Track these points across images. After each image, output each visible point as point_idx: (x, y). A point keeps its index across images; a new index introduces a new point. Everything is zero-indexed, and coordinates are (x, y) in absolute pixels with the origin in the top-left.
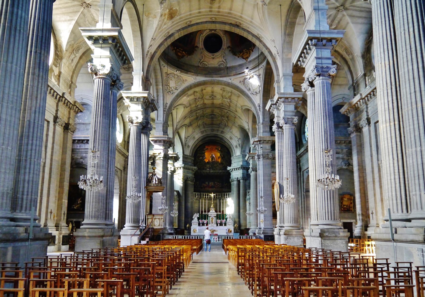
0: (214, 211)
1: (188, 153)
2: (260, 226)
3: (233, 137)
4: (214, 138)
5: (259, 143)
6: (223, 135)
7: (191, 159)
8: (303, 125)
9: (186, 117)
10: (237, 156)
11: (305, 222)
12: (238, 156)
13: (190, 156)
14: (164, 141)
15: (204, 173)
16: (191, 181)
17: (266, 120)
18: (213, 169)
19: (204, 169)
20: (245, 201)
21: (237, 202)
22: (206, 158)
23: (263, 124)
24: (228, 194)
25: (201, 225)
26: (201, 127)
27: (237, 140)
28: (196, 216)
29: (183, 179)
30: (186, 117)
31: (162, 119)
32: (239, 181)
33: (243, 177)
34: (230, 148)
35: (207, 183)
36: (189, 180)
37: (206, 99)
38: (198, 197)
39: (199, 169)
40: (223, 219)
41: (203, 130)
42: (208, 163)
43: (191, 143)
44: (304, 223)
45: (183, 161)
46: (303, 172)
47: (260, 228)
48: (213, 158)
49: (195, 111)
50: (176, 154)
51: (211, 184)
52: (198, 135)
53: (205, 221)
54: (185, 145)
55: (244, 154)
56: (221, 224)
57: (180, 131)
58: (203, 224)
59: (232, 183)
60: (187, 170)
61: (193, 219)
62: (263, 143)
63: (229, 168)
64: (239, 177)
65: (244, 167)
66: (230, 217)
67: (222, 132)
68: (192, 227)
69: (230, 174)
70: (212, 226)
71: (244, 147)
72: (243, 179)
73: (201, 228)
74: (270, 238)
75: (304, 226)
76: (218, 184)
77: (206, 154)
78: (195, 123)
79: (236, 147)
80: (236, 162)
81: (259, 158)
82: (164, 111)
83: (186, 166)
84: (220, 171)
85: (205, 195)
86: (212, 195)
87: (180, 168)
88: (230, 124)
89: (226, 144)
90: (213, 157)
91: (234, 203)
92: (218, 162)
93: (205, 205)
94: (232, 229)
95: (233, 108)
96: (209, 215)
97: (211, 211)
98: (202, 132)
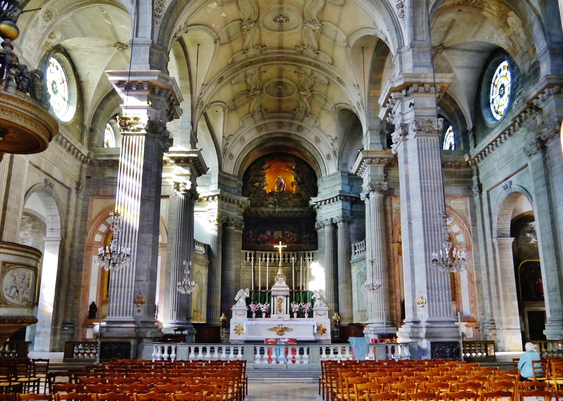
0: (284, 284)
1: (229, 168)
2: (415, 314)
3: (322, 137)
4: (280, 143)
5: (404, 92)
6: (300, 134)
7: (235, 181)
8: (484, 87)
9: (221, 79)
10: (329, 176)
11: (499, 308)
12: (333, 175)
13: (235, 176)
14: (152, 87)
15: (263, 212)
16: (236, 226)
17: (419, 37)
18: (280, 206)
19: (262, 205)
20: (349, 266)
21: (331, 269)
22: (266, 185)
23: (412, 46)
24: (311, 252)
25: (254, 315)
26: (258, 116)
27: (329, 142)
28: (242, 296)
29: (218, 220)
30: (221, 79)
31: (148, 34)
32: (334, 226)
33: (343, 217)
34: (315, 161)
35: (269, 233)
36: (232, 224)
37: (264, 26)
38: (250, 260)
39: (252, 205)
40: (305, 302)
41: (260, 123)
42: (272, 194)
43: (237, 150)
44: (495, 311)
45: (219, 183)
46: (488, 192)
47: (416, 322)
48: (280, 185)
49: (242, 67)
50: (195, 152)
51: (277, 234)
52: (251, 135)
53: (264, 308)
54: (224, 153)
55: (345, 170)
56: (301, 314)
57: (209, 112)
58: (259, 314)
59: (319, 231)
60: (227, 204)
61: (235, 302)
62: (416, 92)
63: (313, 201)
64: (334, 217)
65: (346, 196)
66: (321, 298)
67: (300, 128)
68: (232, 321)
69: (314, 214)
70: (280, 318)
71: (344, 157)
72: (343, 221)
73: (254, 323)
74: (448, 350)
75: (496, 318)
76: (291, 236)
77: (268, 178)
78: (244, 104)
79: (328, 157)
80: (329, 185)
81: (405, 134)
82: (154, 15)
83: (226, 194)
84: (296, 209)
85: (266, 257)
86: (280, 247)
87: (213, 197)
88: (316, 109)
89: (307, 154)
90: (281, 184)
91: (326, 271)
92: (290, 192)
93: (264, 276)
94: (327, 324)
95: (324, 58)
96: (273, 294)
97: (277, 284)
98: (259, 128)
